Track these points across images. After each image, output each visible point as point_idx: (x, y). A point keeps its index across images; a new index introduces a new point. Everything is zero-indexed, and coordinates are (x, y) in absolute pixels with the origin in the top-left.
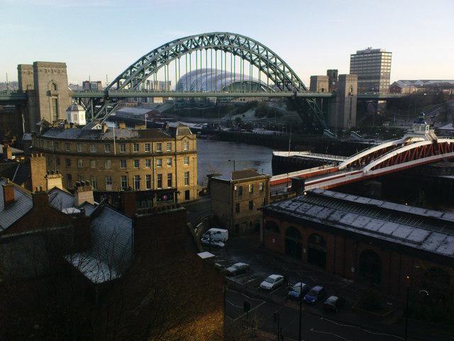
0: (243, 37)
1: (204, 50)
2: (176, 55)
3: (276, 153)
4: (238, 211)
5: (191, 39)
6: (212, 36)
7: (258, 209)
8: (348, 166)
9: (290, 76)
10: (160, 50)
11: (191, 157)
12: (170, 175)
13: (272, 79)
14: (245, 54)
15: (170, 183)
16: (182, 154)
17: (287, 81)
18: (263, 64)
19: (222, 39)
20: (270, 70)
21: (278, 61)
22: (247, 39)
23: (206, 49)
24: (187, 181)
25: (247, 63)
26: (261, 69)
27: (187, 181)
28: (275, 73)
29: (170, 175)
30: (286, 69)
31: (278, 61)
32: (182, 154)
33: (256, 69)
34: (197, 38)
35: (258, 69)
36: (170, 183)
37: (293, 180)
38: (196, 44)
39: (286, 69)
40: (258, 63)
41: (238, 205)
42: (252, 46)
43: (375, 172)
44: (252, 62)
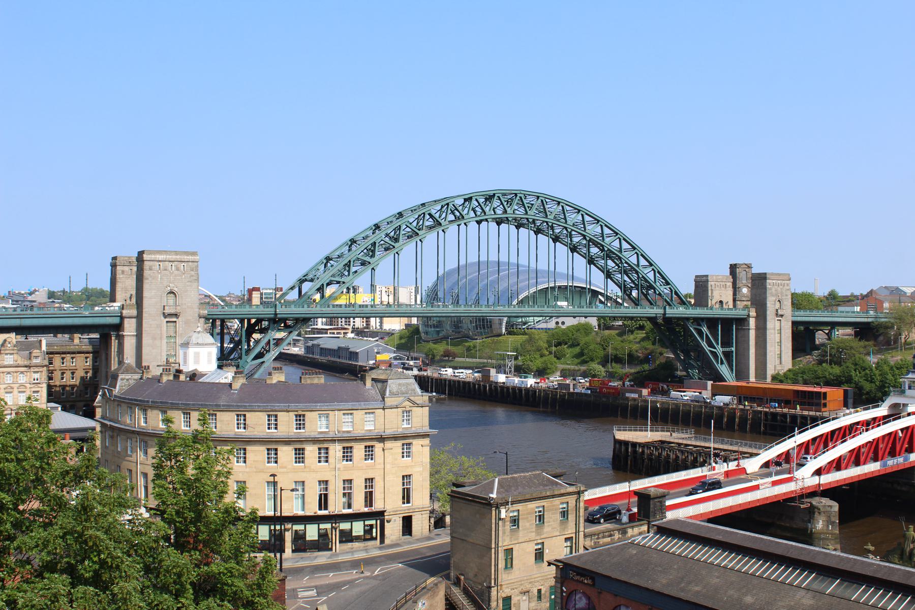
1: (473, 225)
3: (622, 435)
4: (509, 564)
5: (446, 205)
6: (489, 198)
7: (549, 564)
8: (766, 465)
10: (383, 226)
11: (417, 444)
12: (370, 481)
14: (557, 231)
15: (369, 498)
16: (395, 438)
18: (594, 250)
19: (510, 202)
23: (479, 222)
24: (406, 497)
25: (562, 249)
26: (591, 261)
27: (406, 497)
29: (370, 481)
32: (395, 438)
33: (580, 262)
34: (459, 201)
35: (584, 261)
36: (369, 498)
37: (643, 497)
38: (457, 214)
39: (643, 262)
40: (584, 250)
41: (509, 552)
44: (574, 249)
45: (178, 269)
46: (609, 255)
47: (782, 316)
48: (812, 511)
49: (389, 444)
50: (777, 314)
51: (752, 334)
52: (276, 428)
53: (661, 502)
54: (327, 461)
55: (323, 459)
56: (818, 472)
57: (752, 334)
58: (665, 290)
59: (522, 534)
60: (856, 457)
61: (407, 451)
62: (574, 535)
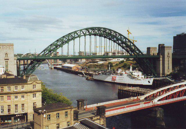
0: (108, 29)
2: (73, 38)
9: (133, 48)
13: (125, 49)
16: (31, 92)
17: (133, 51)
20: (124, 45)
21: (127, 40)
22: (110, 30)
28: (126, 47)
30: (132, 44)
31: (127, 40)
32: (31, 92)
36: (23, 109)
42: (112, 33)
43: (159, 103)
45: (8, 48)
46: (123, 43)
47: (169, 57)
48: (156, 111)
49: (29, 94)
50: (168, 57)
51: (161, 62)
52: (10, 90)
53: (104, 110)
54: (10, 100)
55: (9, 99)
56: (160, 100)
57: (161, 62)
58: (137, 52)
59: (51, 122)
60: (172, 96)
61: (34, 95)
62: (70, 121)
